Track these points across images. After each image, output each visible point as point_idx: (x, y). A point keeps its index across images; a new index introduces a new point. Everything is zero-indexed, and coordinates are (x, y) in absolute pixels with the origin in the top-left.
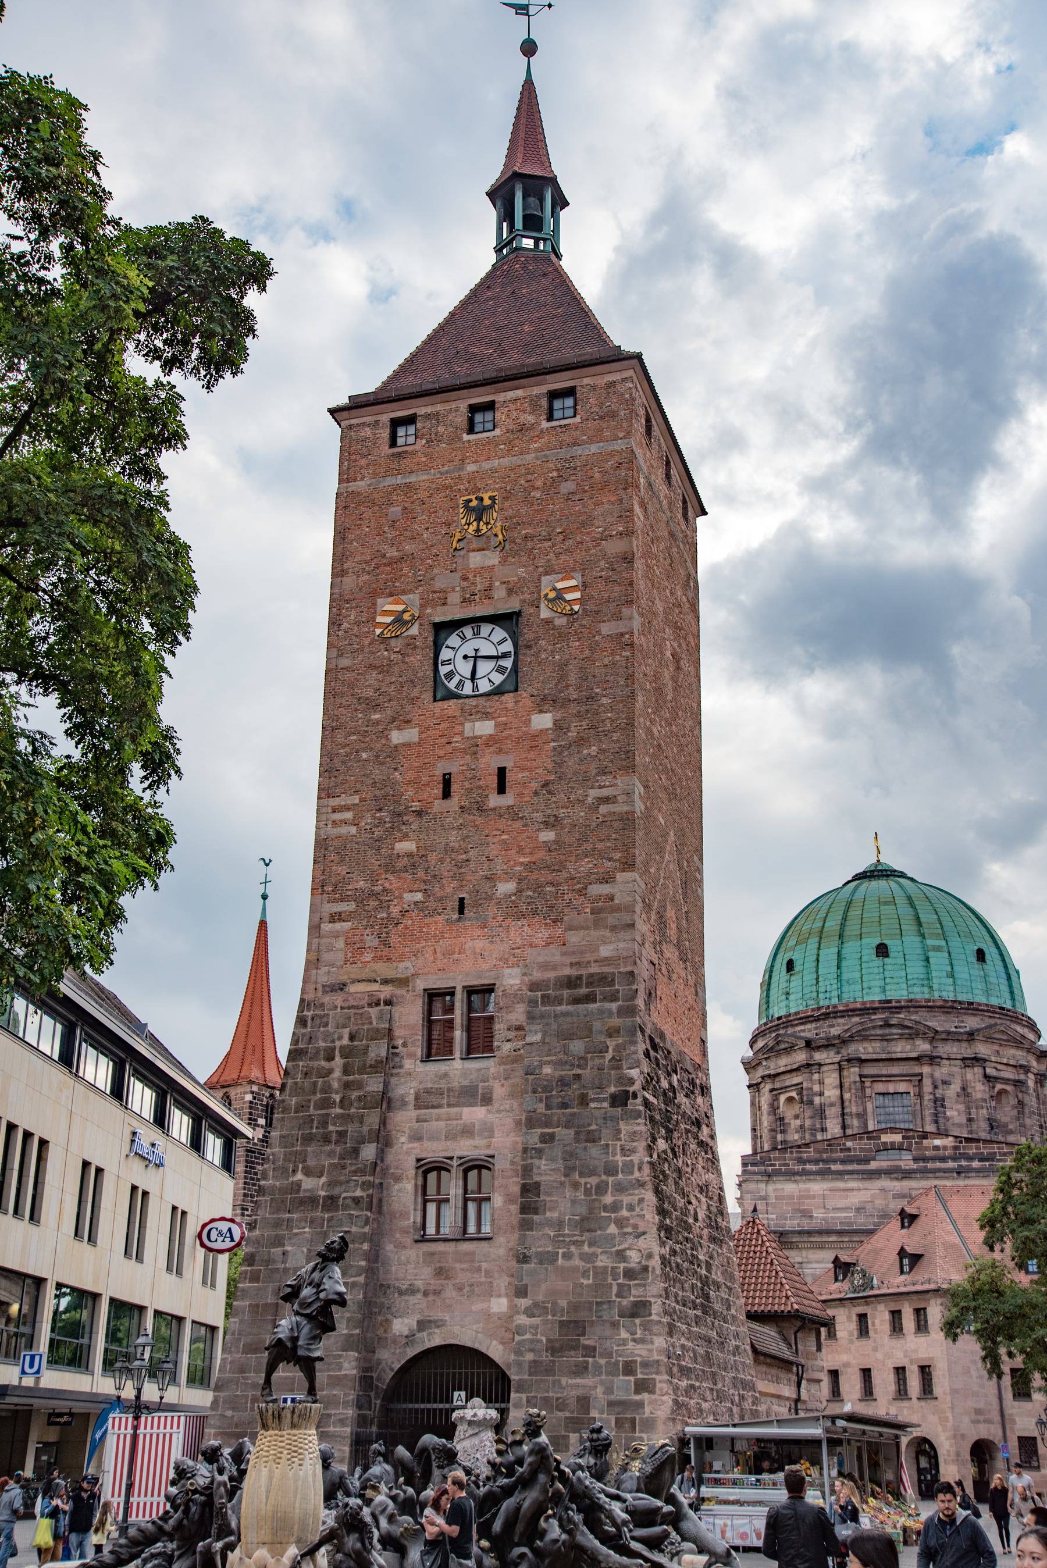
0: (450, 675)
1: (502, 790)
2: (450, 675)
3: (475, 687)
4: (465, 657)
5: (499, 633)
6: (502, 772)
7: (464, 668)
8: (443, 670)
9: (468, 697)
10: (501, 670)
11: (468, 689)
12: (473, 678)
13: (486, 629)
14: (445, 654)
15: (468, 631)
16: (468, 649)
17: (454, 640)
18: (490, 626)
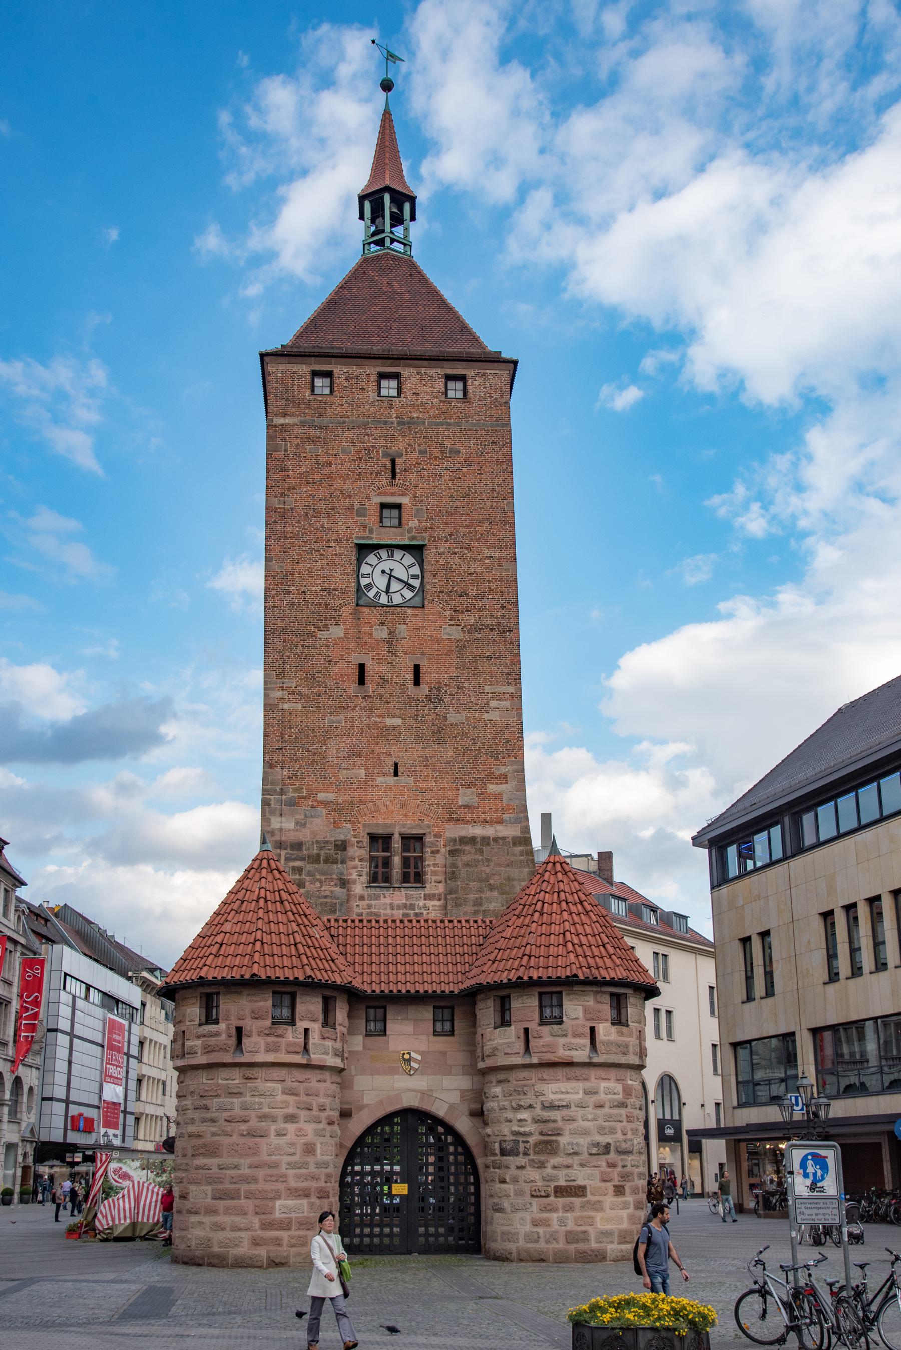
0: (369, 587)
1: (417, 682)
2: (369, 587)
3: (390, 600)
4: (383, 572)
5: (409, 559)
6: (417, 669)
7: (381, 582)
8: (364, 582)
9: (383, 606)
10: (411, 587)
11: (384, 600)
12: (387, 591)
13: (398, 554)
14: (365, 569)
15: (384, 553)
16: (386, 566)
17: (372, 559)
18: (403, 552)
